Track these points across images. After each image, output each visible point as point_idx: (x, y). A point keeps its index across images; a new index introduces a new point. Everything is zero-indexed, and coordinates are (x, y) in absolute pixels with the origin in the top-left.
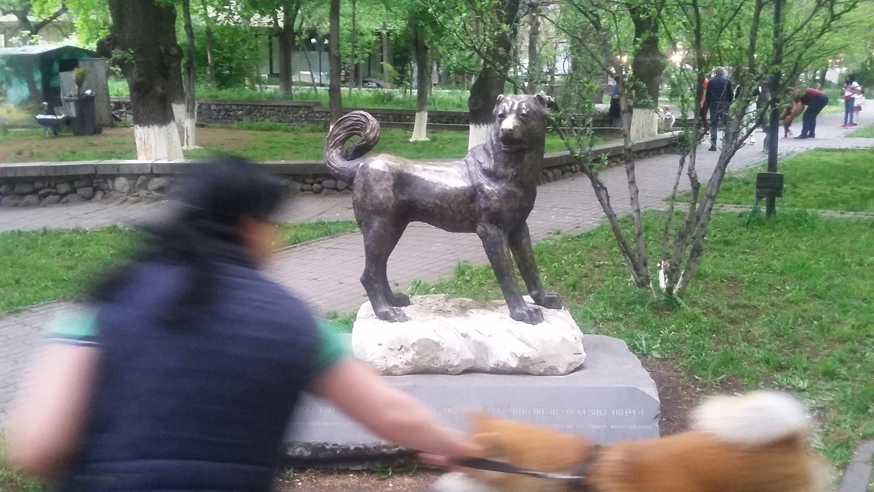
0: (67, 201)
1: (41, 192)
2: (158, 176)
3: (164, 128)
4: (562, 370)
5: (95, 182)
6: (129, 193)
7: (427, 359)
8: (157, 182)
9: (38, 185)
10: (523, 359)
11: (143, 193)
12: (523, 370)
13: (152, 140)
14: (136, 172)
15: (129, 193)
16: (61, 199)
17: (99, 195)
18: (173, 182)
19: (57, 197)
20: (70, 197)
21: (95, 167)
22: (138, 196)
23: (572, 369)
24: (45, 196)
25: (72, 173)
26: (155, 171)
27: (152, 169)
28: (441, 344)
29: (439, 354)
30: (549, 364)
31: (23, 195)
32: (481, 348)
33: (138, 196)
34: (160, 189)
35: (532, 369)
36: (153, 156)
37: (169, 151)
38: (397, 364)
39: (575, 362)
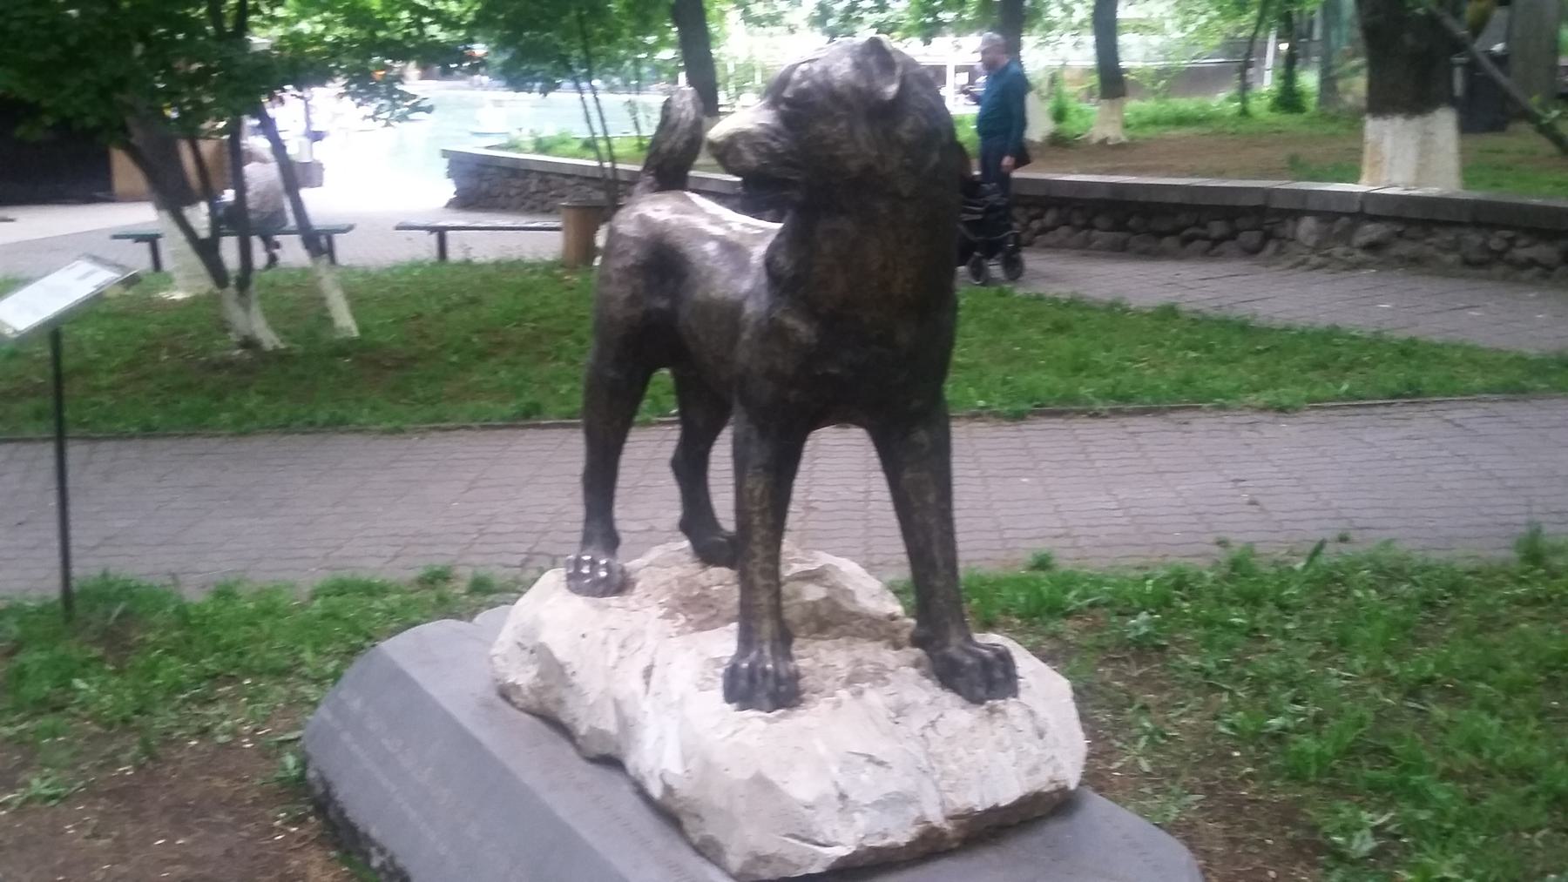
0: (1219, 254)
2: (1374, 219)
3: (1417, 122)
5: (1267, 221)
6: (1315, 249)
8: (1371, 231)
9: (1182, 219)
10: (668, 790)
11: (1339, 250)
13: (1388, 145)
14: (1334, 208)
15: (1315, 249)
16: (1212, 248)
17: (1271, 247)
18: (1400, 235)
19: (1206, 244)
20: (1227, 246)
21: (1268, 193)
22: (1328, 255)
25: (1229, 202)
26: (1369, 210)
27: (1362, 203)
28: (569, 672)
29: (564, 692)
31: (1161, 235)
33: (1328, 255)
34: (1372, 247)
35: (689, 824)
36: (1385, 178)
37: (1422, 170)
38: (519, 683)
39: (783, 860)
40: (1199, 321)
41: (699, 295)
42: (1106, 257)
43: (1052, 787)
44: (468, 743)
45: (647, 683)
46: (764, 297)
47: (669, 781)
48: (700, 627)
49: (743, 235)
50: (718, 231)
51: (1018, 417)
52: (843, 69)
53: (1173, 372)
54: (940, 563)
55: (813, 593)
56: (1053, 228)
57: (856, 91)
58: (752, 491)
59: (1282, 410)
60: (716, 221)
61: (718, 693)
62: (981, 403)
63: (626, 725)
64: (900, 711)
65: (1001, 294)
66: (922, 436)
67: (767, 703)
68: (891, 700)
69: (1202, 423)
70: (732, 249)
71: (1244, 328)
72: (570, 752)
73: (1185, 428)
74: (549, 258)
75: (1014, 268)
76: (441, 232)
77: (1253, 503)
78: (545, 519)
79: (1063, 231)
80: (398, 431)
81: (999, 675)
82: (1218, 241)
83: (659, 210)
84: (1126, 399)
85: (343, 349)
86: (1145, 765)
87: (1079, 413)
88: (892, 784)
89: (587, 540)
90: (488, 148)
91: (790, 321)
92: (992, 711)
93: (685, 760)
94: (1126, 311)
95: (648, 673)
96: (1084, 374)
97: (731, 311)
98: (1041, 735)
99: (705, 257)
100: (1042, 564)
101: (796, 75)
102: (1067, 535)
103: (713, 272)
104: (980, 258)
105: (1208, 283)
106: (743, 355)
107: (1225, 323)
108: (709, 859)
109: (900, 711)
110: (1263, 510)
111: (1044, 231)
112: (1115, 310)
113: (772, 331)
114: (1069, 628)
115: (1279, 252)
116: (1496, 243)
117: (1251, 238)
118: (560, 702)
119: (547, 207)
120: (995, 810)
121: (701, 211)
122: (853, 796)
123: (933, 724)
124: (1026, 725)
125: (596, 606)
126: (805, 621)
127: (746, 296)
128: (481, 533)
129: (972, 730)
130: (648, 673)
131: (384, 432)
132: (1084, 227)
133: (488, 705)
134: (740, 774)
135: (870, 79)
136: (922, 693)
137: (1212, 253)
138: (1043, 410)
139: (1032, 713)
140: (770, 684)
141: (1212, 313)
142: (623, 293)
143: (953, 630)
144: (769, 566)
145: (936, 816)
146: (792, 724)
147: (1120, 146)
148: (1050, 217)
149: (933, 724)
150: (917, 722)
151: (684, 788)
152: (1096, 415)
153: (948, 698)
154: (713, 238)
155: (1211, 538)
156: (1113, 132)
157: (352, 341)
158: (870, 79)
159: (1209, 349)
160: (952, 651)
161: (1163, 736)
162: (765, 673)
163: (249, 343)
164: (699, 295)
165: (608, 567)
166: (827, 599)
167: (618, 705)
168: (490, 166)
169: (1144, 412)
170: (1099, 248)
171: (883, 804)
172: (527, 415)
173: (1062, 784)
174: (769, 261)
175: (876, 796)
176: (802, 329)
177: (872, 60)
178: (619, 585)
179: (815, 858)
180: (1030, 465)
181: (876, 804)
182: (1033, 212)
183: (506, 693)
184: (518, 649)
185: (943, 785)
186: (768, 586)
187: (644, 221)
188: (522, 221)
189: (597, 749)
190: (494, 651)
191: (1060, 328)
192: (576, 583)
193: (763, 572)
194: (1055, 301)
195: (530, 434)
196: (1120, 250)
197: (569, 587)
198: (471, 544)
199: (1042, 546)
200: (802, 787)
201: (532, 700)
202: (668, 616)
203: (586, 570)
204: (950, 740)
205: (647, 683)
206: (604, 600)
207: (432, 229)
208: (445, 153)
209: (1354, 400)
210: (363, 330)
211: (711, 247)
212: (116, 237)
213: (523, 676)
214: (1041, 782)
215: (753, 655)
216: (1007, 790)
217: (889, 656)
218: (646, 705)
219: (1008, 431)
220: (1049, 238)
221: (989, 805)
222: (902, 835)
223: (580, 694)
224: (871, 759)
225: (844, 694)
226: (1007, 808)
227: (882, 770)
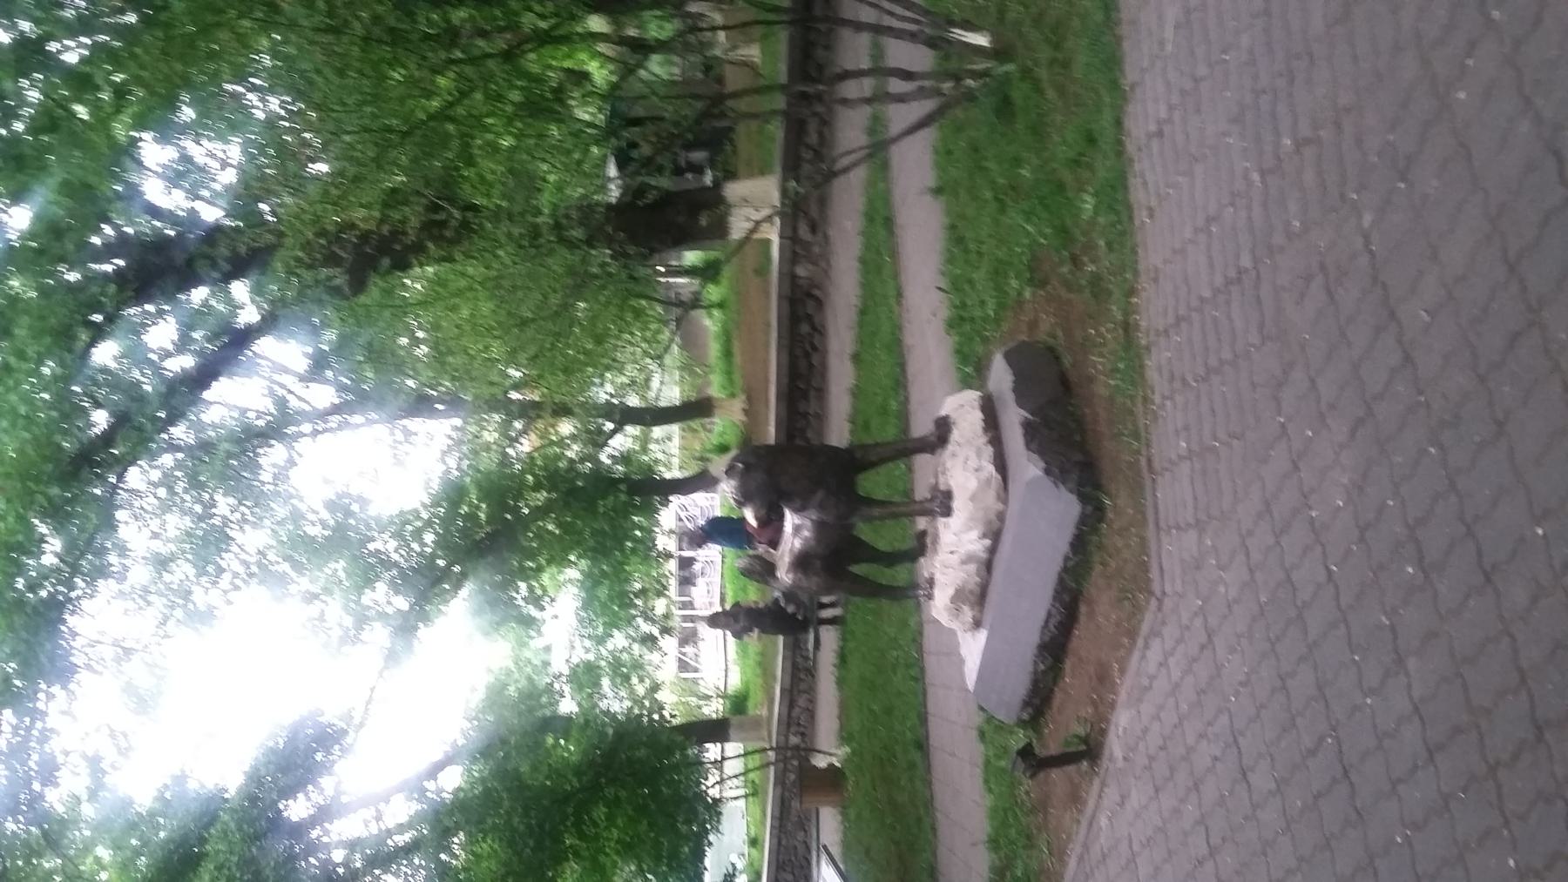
0: (823, 326)
2: (795, 229)
4: (1000, 506)
6: (815, 264)
10: (984, 536)
11: (816, 249)
12: (994, 535)
17: (816, 292)
19: (817, 336)
20: (817, 320)
21: (780, 297)
24: (815, 349)
30: (993, 517)
31: (811, 366)
32: (968, 559)
34: (814, 228)
35: (996, 524)
40: (860, 340)
44: (991, 627)
52: (733, 483)
59: (900, 295)
66: (858, 455)
69: (909, 340)
70: (797, 529)
71: (863, 312)
74: (839, 818)
80: (934, 829)
82: (814, 328)
88: (973, 455)
93: (970, 529)
95: (952, 553)
107: (861, 325)
112: (856, 393)
113: (821, 507)
115: (818, 287)
116: (807, 155)
117: (810, 307)
118: (971, 592)
119: (804, 863)
120: (985, 421)
127: (812, 520)
136: (950, 447)
147: (750, 399)
176: (820, 495)
189: (984, 573)
195: (931, 742)
196: (822, 392)
200: (973, 484)
209: (894, 254)
214: (976, 404)
216: (978, 416)
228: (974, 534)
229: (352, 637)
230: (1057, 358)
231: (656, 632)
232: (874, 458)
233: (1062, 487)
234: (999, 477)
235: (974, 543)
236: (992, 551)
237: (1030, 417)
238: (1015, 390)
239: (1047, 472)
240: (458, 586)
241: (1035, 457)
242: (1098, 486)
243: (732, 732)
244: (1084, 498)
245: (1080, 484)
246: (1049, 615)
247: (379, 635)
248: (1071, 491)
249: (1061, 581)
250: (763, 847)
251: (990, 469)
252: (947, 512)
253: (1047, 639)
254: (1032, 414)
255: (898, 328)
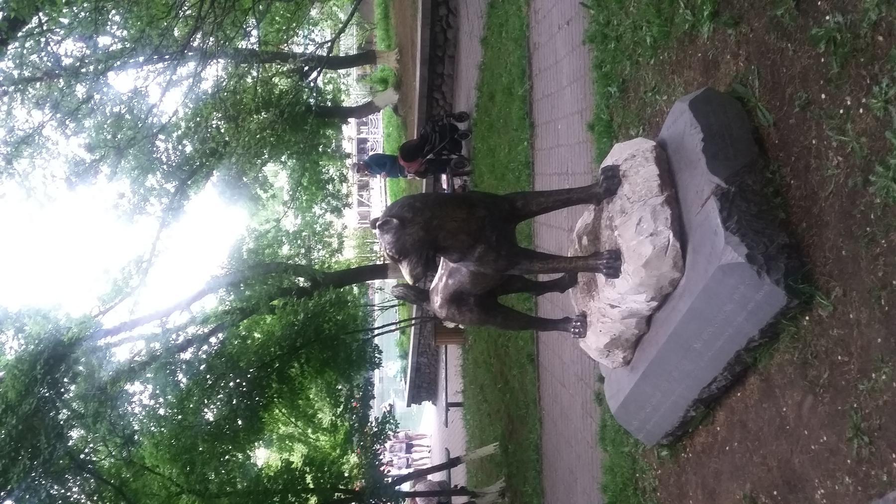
0: (456, 9)
1: (445, 27)
4: (677, 275)
7: (625, 344)
9: (438, 29)
10: (653, 299)
12: (663, 299)
16: (452, 13)
19: (451, 16)
23: (680, 263)
24: (449, 26)
29: (623, 338)
31: (446, 39)
35: (665, 292)
40: (488, 27)
41: (468, 286)
42: (457, 65)
43: (654, 152)
44: (644, 376)
45: (616, 307)
46: (468, 264)
47: (649, 299)
48: (597, 286)
49: (445, 270)
50: (444, 279)
51: (532, 126)
52: (388, 237)
53: (511, 46)
54: (568, 196)
55: (585, 241)
56: (443, 93)
57: (395, 234)
58: (540, 268)
60: (440, 279)
61: (616, 280)
62: (526, 143)
63: (631, 315)
64: (623, 212)
65: (475, 125)
66: (519, 204)
67: (618, 263)
68: (619, 215)
70: (450, 275)
72: (646, 336)
73: (537, 46)
74: (460, 351)
75: (462, 117)
76: (449, 405)
77: (568, 24)
78: (576, 351)
79: (444, 89)
81: (610, 173)
82: (449, 10)
83: (437, 301)
84: (524, 72)
85: (504, 449)
86: (665, 98)
87: (531, 96)
89: (567, 330)
90: (406, 382)
91: (476, 255)
92: (624, 176)
94: (483, 63)
95: (613, 307)
96: (513, 90)
97: (474, 275)
98: (635, 156)
99: (453, 283)
100: (591, 127)
101: (390, 254)
102: (581, 113)
103: (459, 281)
104: (458, 135)
105: (470, 18)
106: (489, 271)
107: (489, 16)
108: (678, 284)
109: (623, 212)
110: (571, 20)
111: (444, 98)
112: (483, 68)
113: (480, 260)
114: (618, 120)
118: (627, 340)
119: (435, 353)
120: (660, 176)
121: (437, 284)
122: (651, 231)
123: (628, 199)
124: (630, 163)
125: (591, 325)
126: (595, 245)
127: (468, 270)
128: (582, 380)
129: (630, 184)
130: (613, 307)
131: (541, 427)
132: (443, 78)
133: (632, 369)
134: (643, 273)
135: (392, 228)
136: (618, 203)
137: (455, 12)
138: (529, 113)
139: (626, 160)
140: (611, 261)
141: (484, 20)
142: (468, 315)
143: (593, 190)
144: (568, 260)
145: (661, 199)
146: (626, 254)
147: (401, 52)
148: (437, 96)
149: (628, 199)
150: (628, 205)
151: (651, 294)
152: (532, 87)
153: (620, 192)
154: (447, 280)
155: (582, 47)
156: (393, 56)
157: (501, 445)
158: (392, 228)
159: (501, 25)
160: (601, 190)
161: (654, 88)
162: (607, 263)
163: (502, 494)
164: (468, 286)
165: (576, 322)
166: (587, 236)
167: (624, 318)
168: (415, 381)
169: (530, 64)
170: (453, 70)
171: (655, 220)
172: (532, 360)
173: (653, 148)
174: (454, 262)
175: (652, 222)
176: (479, 250)
177: (385, 228)
178: (584, 316)
179: (674, 246)
180: (553, 123)
181: (655, 222)
182: (435, 105)
183: (627, 362)
184: (608, 358)
185: (650, 196)
186: (576, 261)
187: (441, 307)
188: (443, 365)
189: (644, 326)
190: (611, 367)
191: (492, 98)
192: (582, 334)
193: (570, 263)
194: (479, 98)
195: (541, 359)
196: (454, 59)
197: (584, 337)
198: (586, 384)
199: (585, 127)
200: (647, 250)
201: (628, 351)
202: (593, 297)
203: (577, 330)
204: (634, 193)
205: (616, 307)
206: (588, 324)
207: (447, 410)
208: (409, 405)
210: (495, 440)
211: (450, 282)
212: (446, 425)
213: (619, 356)
214: (651, 156)
215: (601, 267)
216: (653, 170)
217: (605, 215)
218: (624, 307)
219: (539, 131)
220: (448, 96)
221: (657, 178)
222: (667, 212)
223: (622, 332)
224: (638, 224)
225: (616, 233)
226: (660, 170)
227: (643, 220)
228: (643, 297)
229: (139, 208)
230: (750, 113)
231: (340, 205)
232: (534, 208)
233: (767, 280)
234: (678, 245)
235: (641, 303)
236: (658, 308)
237: (723, 185)
238: (705, 150)
239: (750, 258)
240: (209, 175)
241: (736, 239)
242: (808, 278)
243: (390, 273)
244: (791, 291)
245: (786, 276)
246: (715, 380)
247: (156, 206)
248: (777, 283)
249: (738, 355)
250: (410, 335)
251: (668, 235)
252: (614, 272)
253: (705, 396)
254: (726, 183)
255: (525, 29)
